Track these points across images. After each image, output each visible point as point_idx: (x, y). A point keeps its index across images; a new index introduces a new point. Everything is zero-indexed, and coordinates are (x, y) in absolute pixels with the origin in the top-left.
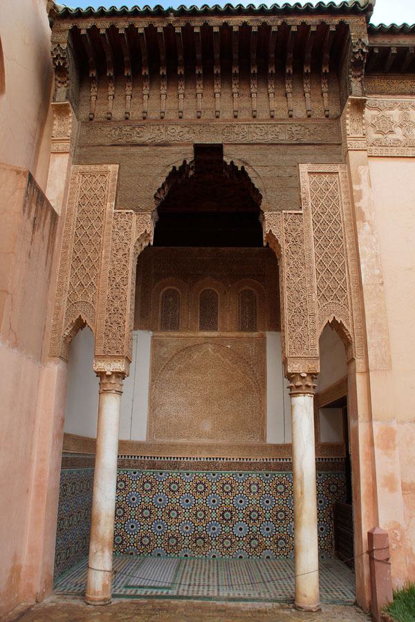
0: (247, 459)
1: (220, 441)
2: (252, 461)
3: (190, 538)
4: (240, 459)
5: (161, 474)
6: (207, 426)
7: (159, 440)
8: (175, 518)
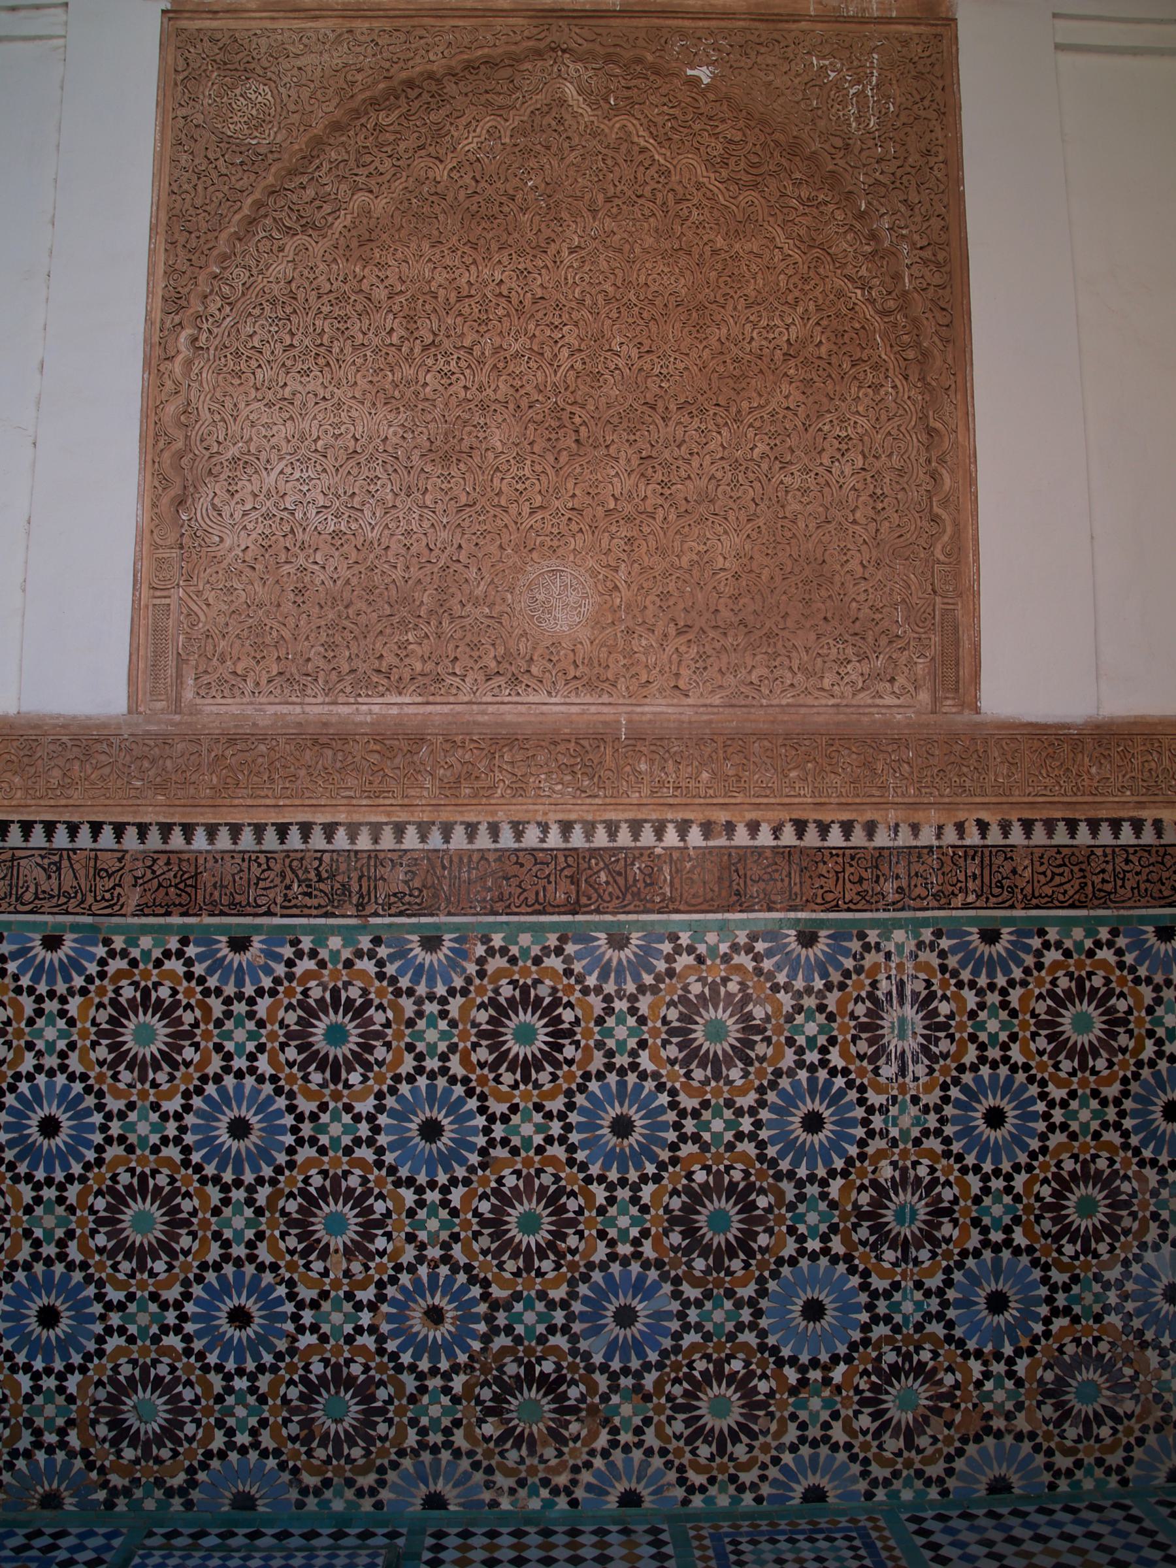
0: (847, 828)
1: (659, 708)
2: (882, 839)
3: (458, 1383)
4: (800, 827)
5: (239, 944)
6: (563, 603)
7: (221, 710)
8: (349, 1253)
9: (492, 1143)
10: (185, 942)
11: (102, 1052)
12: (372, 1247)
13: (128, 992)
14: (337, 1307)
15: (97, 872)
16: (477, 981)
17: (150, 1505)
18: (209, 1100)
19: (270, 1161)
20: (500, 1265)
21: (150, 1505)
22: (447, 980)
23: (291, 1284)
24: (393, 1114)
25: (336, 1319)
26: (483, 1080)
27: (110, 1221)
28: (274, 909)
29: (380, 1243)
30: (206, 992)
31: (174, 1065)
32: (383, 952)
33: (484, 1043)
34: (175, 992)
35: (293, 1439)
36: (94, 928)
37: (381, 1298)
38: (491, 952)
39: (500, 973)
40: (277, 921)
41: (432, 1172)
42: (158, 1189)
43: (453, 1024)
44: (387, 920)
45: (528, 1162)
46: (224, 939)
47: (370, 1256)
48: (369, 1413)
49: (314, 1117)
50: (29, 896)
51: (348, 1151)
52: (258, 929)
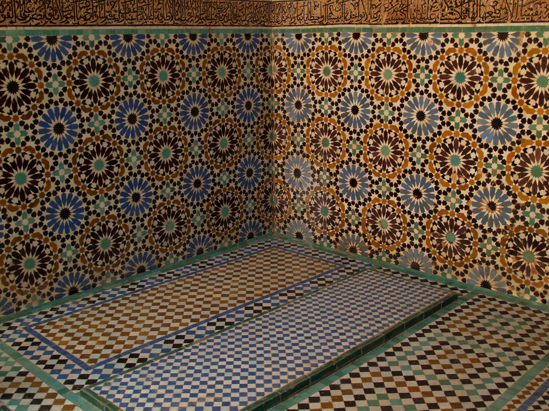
3: (499, 237)
5: (424, 36)
8: (459, 174)
9: (523, 132)
10: (403, 35)
11: (373, 81)
12: (469, 173)
13: (382, 57)
14: (454, 196)
15: (372, 5)
16: (522, 55)
17: (384, 259)
18: (410, 103)
19: (432, 131)
20: (522, 189)
21: (384, 259)
22: (509, 54)
23: (437, 183)
24: (481, 115)
25: (453, 200)
26: (521, 103)
27: (374, 149)
28: (439, 20)
29: (472, 171)
30: (410, 57)
31: (398, 88)
32: (482, 40)
33: (523, 85)
34: (399, 57)
35: (435, 246)
36: (371, 30)
37: (471, 195)
38: (530, 41)
39: (533, 51)
40: (439, 26)
41: (496, 143)
42: (391, 138)
43: (510, 75)
44: (484, 25)
45: (539, 143)
46: (418, 34)
47: (468, 176)
48: (463, 242)
49: (449, 113)
50: (348, 17)
51: (462, 129)
52: (431, 29)
